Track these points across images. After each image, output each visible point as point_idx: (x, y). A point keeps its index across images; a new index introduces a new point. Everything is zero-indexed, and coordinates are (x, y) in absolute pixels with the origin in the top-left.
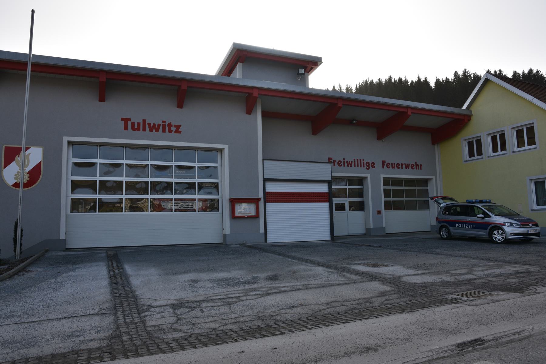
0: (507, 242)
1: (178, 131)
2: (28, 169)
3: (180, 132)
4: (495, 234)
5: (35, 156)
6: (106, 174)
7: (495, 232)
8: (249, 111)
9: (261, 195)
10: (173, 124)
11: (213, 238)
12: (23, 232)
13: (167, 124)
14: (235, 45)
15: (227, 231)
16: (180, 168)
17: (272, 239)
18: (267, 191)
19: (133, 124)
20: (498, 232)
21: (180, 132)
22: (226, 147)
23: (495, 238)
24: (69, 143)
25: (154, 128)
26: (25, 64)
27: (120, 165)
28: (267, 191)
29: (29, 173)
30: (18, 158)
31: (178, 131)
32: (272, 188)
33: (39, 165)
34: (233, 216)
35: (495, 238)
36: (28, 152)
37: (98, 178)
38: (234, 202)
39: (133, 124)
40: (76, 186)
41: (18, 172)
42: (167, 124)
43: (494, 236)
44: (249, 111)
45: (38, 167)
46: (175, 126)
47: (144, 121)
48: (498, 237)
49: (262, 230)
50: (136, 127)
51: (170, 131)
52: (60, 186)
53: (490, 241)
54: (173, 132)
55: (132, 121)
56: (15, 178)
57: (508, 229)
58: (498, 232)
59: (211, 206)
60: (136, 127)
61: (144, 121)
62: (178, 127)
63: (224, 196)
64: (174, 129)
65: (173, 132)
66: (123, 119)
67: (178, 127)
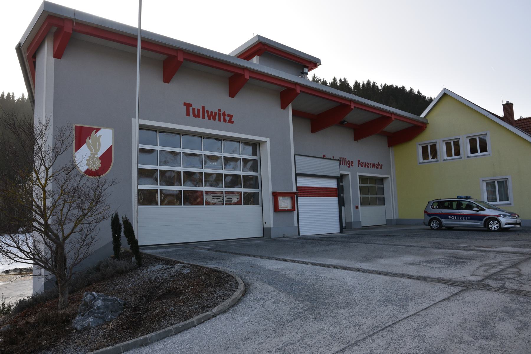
0: (502, 230)
1: (231, 122)
2: (100, 154)
3: (232, 122)
4: (491, 224)
5: (105, 138)
6: (165, 163)
7: (491, 222)
8: (284, 106)
9: (294, 190)
10: (227, 113)
11: (253, 231)
12: (139, 223)
13: (222, 113)
14: (258, 36)
15: (270, 223)
16: (208, 157)
17: (303, 232)
18: (298, 185)
19: (194, 109)
20: (494, 222)
21: (232, 122)
22: (267, 140)
23: (491, 227)
24: (142, 128)
25: (212, 116)
26: (136, 39)
27: (178, 154)
28: (298, 185)
29: (101, 158)
30: (89, 141)
31: (231, 122)
32: (304, 182)
33: (110, 150)
34: (276, 209)
35: (491, 227)
36: (99, 133)
37: (159, 168)
38: (276, 195)
39: (194, 109)
40: (143, 174)
41: (90, 157)
42: (222, 113)
43: (490, 226)
44: (284, 106)
45: (109, 151)
46: (229, 116)
47: (203, 108)
48: (494, 226)
49: (296, 225)
50: (196, 113)
51: (225, 121)
52: (131, 174)
53: (486, 229)
54: (227, 121)
55: (193, 107)
56: (87, 164)
57: (503, 220)
58: (494, 222)
59: (252, 199)
60: (196, 113)
61: (203, 108)
62: (231, 116)
63: (267, 188)
64: (227, 118)
65: (227, 121)
66: (185, 104)
67: (231, 116)
